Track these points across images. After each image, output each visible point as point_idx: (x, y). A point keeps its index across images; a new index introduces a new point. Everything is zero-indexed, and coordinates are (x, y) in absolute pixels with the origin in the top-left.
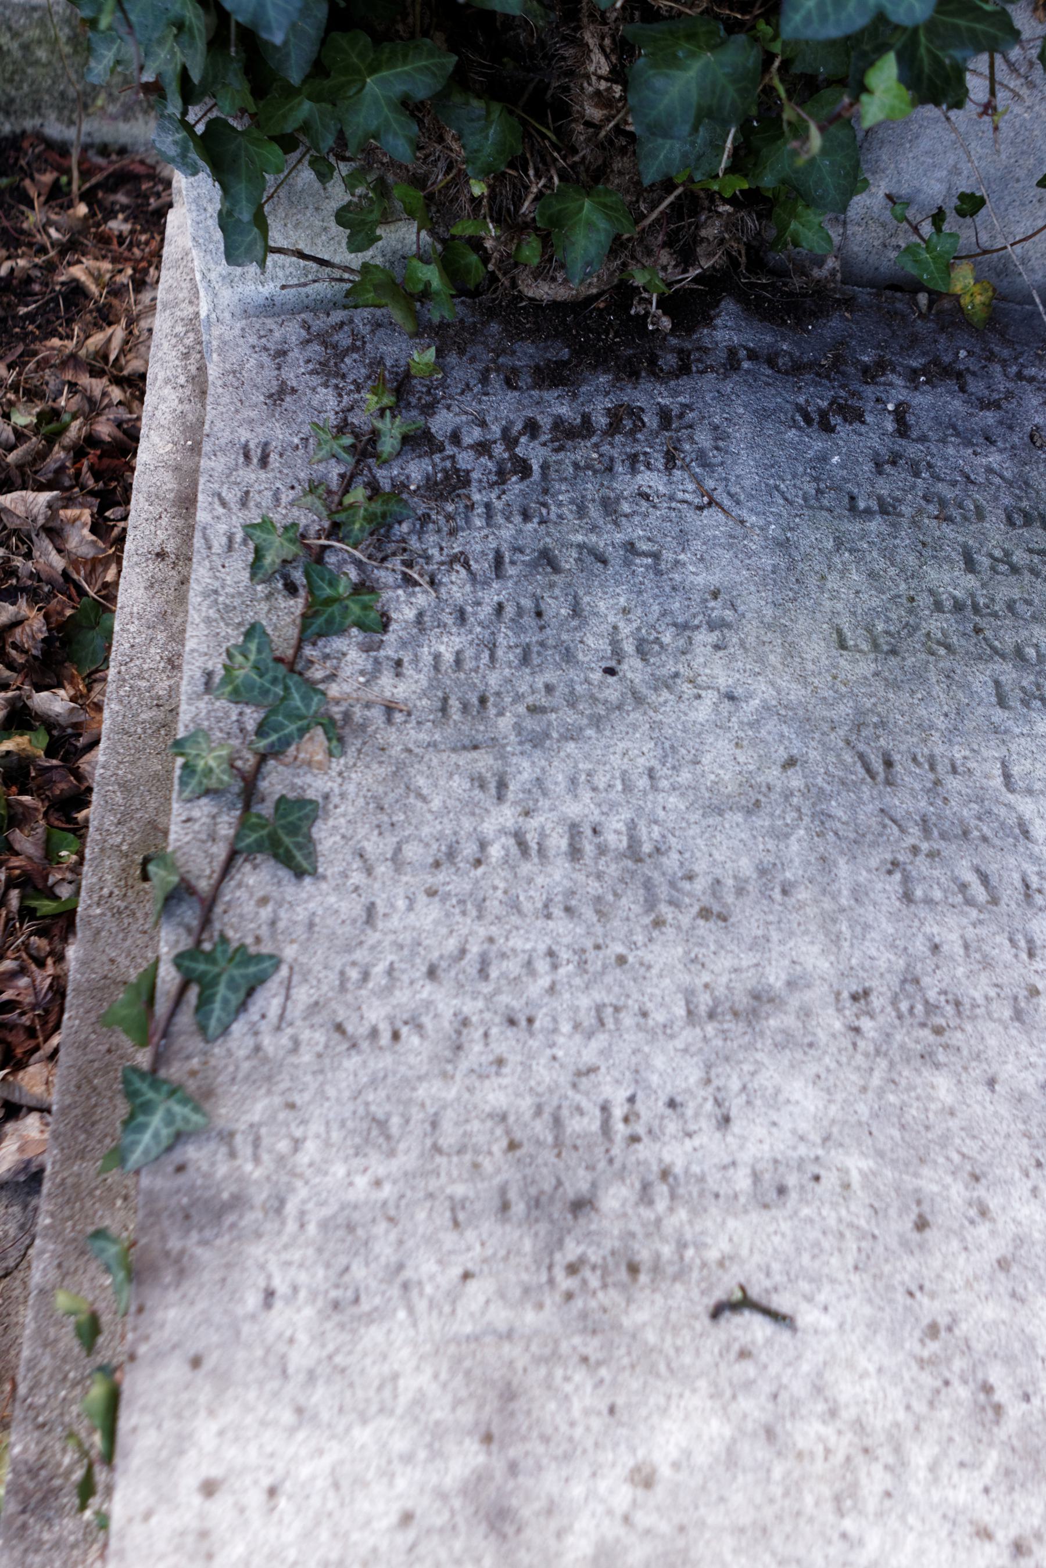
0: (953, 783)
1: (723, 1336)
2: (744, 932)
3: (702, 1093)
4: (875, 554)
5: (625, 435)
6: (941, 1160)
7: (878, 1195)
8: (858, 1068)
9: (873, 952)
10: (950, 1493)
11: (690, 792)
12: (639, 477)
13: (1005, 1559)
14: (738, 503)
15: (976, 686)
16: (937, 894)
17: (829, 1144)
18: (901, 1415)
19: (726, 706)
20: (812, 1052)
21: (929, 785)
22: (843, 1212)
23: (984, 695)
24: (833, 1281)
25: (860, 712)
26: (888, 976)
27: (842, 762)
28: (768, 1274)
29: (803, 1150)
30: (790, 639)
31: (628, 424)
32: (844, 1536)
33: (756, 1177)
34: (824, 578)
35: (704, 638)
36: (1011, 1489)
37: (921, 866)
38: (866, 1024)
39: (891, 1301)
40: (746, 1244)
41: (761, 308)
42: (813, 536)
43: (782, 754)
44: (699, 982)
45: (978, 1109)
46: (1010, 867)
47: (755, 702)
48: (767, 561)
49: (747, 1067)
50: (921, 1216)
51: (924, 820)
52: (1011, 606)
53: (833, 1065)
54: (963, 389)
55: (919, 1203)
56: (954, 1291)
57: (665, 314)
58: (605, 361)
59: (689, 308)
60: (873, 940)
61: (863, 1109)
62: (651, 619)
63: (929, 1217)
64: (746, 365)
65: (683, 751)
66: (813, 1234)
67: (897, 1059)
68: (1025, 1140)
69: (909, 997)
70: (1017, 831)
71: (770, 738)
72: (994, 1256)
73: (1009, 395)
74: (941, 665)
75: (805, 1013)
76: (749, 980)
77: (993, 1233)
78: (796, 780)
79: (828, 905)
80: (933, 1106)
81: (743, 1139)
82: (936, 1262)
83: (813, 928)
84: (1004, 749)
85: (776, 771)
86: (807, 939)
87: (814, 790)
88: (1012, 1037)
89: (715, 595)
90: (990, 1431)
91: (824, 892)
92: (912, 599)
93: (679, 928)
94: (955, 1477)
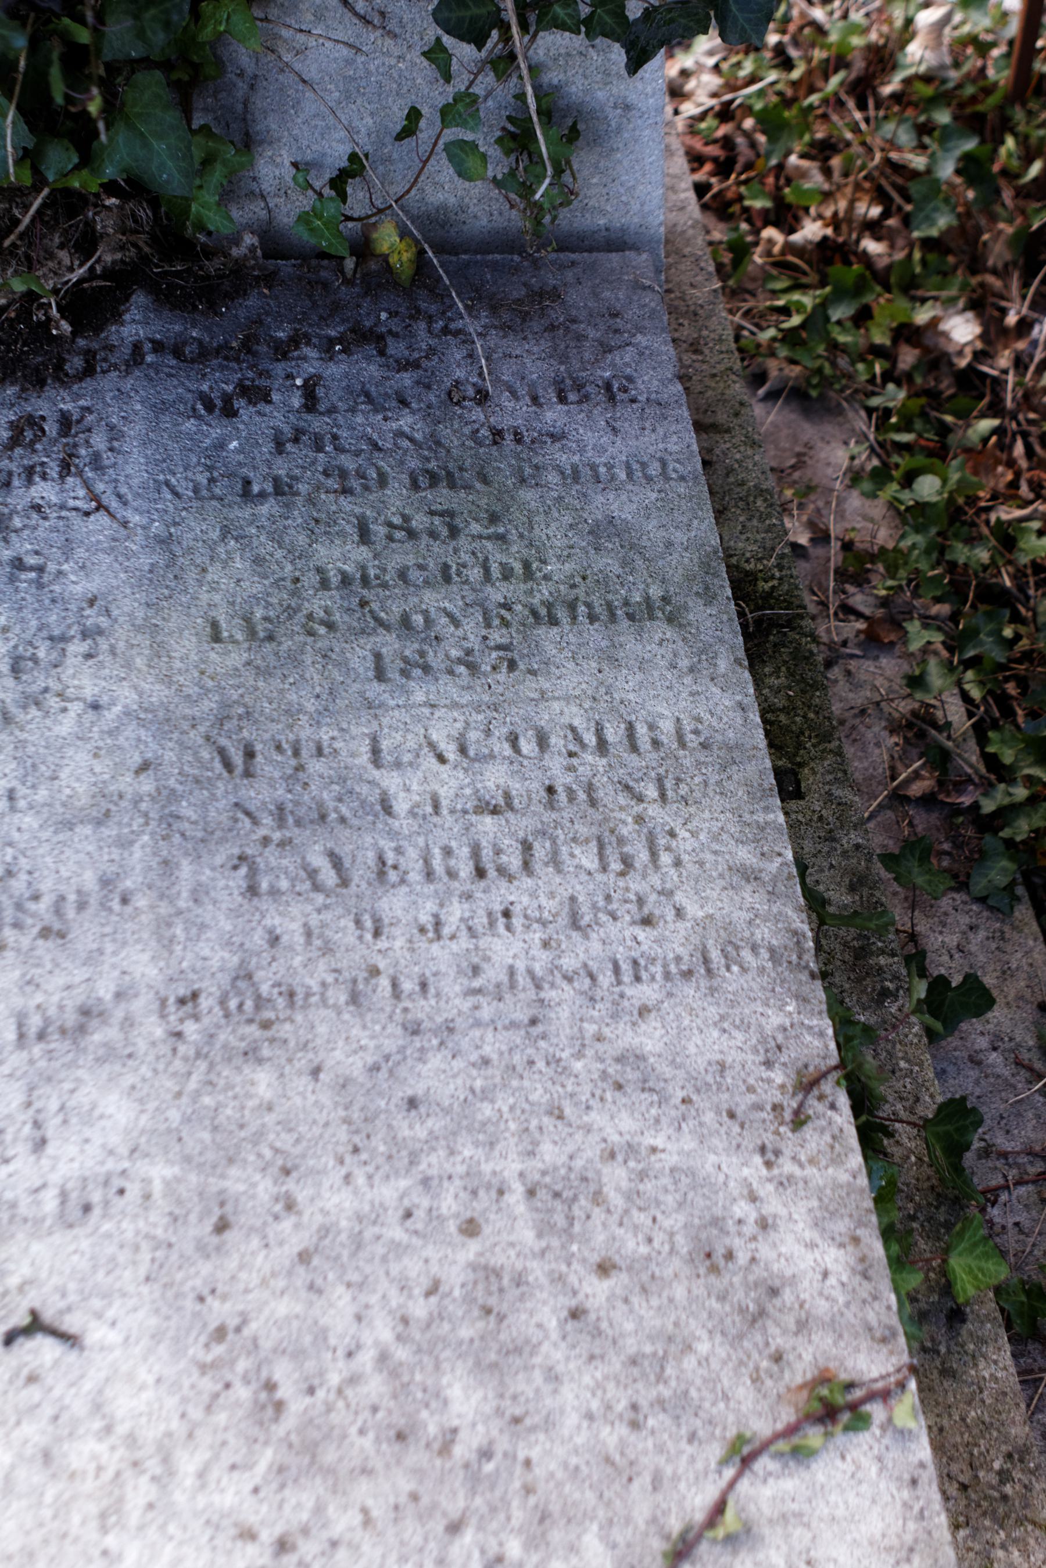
0: (316, 767)
1: (14, 1363)
2: (79, 946)
3: (22, 1117)
4: (263, 539)
5: (24, 447)
6: (252, 1158)
7: (179, 1202)
8: (175, 1074)
9: (206, 952)
10: (216, 1498)
11: (46, 809)
12: (33, 489)
13: (266, 1559)
14: (125, 504)
15: (355, 663)
16: (284, 884)
17: (136, 1155)
18: (175, 1424)
19: (91, 715)
20: (130, 1062)
21: (289, 772)
22: (141, 1224)
23: (361, 670)
24: (124, 1295)
25: (225, 705)
26: (219, 975)
27: (199, 760)
28: (64, 1295)
29: (110, 1165)
30: (159, 639)
31: (29, 434)
32: (105, 1553)
33: (64, 1196)
34: (204, 570)
35: (77, 647)
36: (282, 1486)
37: (271, 856)
38: (190, 1028)
39: (179, 1309)
40: (46, 1266)
41: (169, 298)
42: (199, 528)
43: (137, 759)
44: (33, 1003)
45: (298, 1101)
46: (363, 848)
47: (117, 709)
48: (145, 561)
49: (67, 1086)
50: (222, 1218)
51: (281, 808)
52: (403, 575)
53: (149, 1074)
54: (382, 353)
55: (222, 1204)
56: (247, 1291)
57: (63, 317)
58: (14, 372)
59: (92, 308)
60: (208, 940)
61: (174, 1116)
62: (28, 636)
63: (231, 1218)
64: (149, 359)
65: (43, 768)
66: (110, 1249)
67: (218, 1059)
68: (345, 1127)
69: (239, 993)
70: (378, 807)
71: (126, 744)
72: (296, 1250)
73: (431, 351)
74: (319, 645)
75: (128, 1023)
76: (79, 996)
77: (297, 1226)
78: (147, 785)
79: (164, 909)
80: (250, 1104)
81: (56, 1159)
82: (232, 1264)
83: (145, 935)
84: (375, 725)
85: (129, 778)
86: (139, 947)
87: (165, 792)
88: (344, 1022)
89: (92, 602)
90: (267, 1430)
91: (162, 896)
92: (297, 580)
93: (18, 951)
94: (224, 1482)
